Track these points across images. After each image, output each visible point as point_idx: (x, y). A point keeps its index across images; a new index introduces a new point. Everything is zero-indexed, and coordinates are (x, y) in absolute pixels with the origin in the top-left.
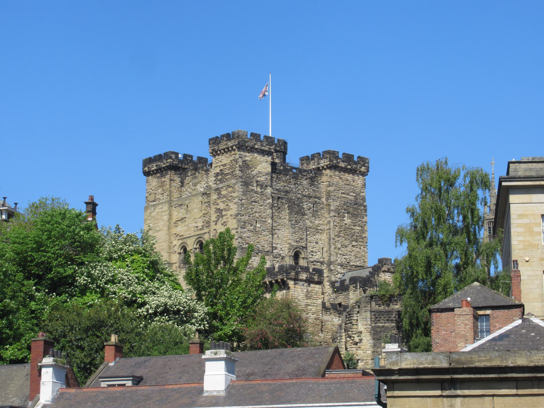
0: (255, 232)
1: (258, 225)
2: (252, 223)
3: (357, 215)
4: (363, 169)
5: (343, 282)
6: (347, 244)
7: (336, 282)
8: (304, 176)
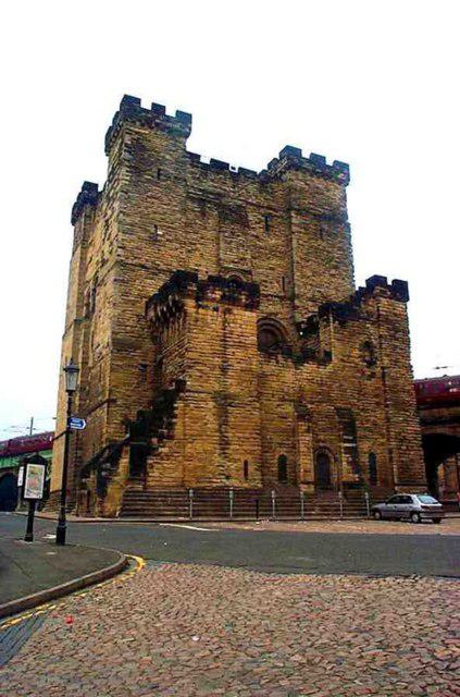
0: (154, 239)
4: (340, 176)
5: (310, 319)
7: (303, 322)
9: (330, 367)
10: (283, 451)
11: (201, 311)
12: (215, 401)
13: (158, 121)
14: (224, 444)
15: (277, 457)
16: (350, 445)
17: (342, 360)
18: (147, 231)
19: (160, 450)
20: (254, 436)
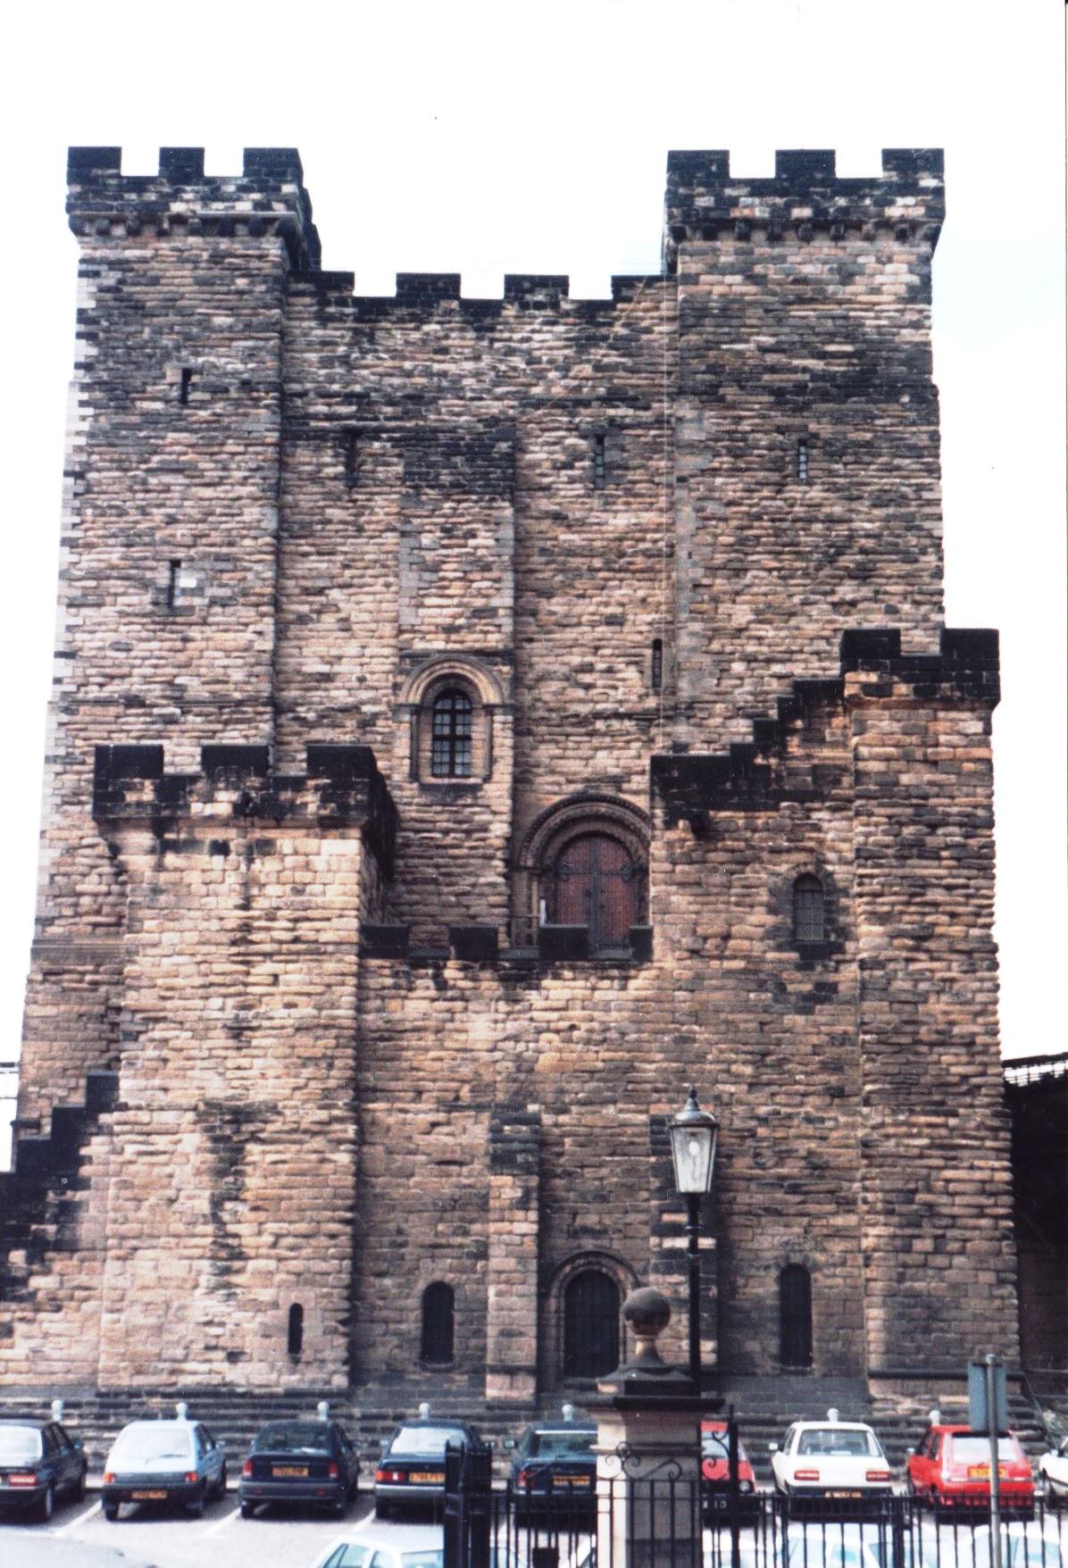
1: (187, 580)
2: (149, 575)
3: (868, 444)
6: (796, 599)
8: (539, 306)
9: (641, 983)
10: (441, 1270)
11: (171, 859)
12: (207, 1130)
13: (177, 207)
14: (229, 1255)
15: (421, 1285)
16: (682, 1243)
17: (694, 953)
18: (145, 585)
19: (35, 1282)
20: (334, 1227)
